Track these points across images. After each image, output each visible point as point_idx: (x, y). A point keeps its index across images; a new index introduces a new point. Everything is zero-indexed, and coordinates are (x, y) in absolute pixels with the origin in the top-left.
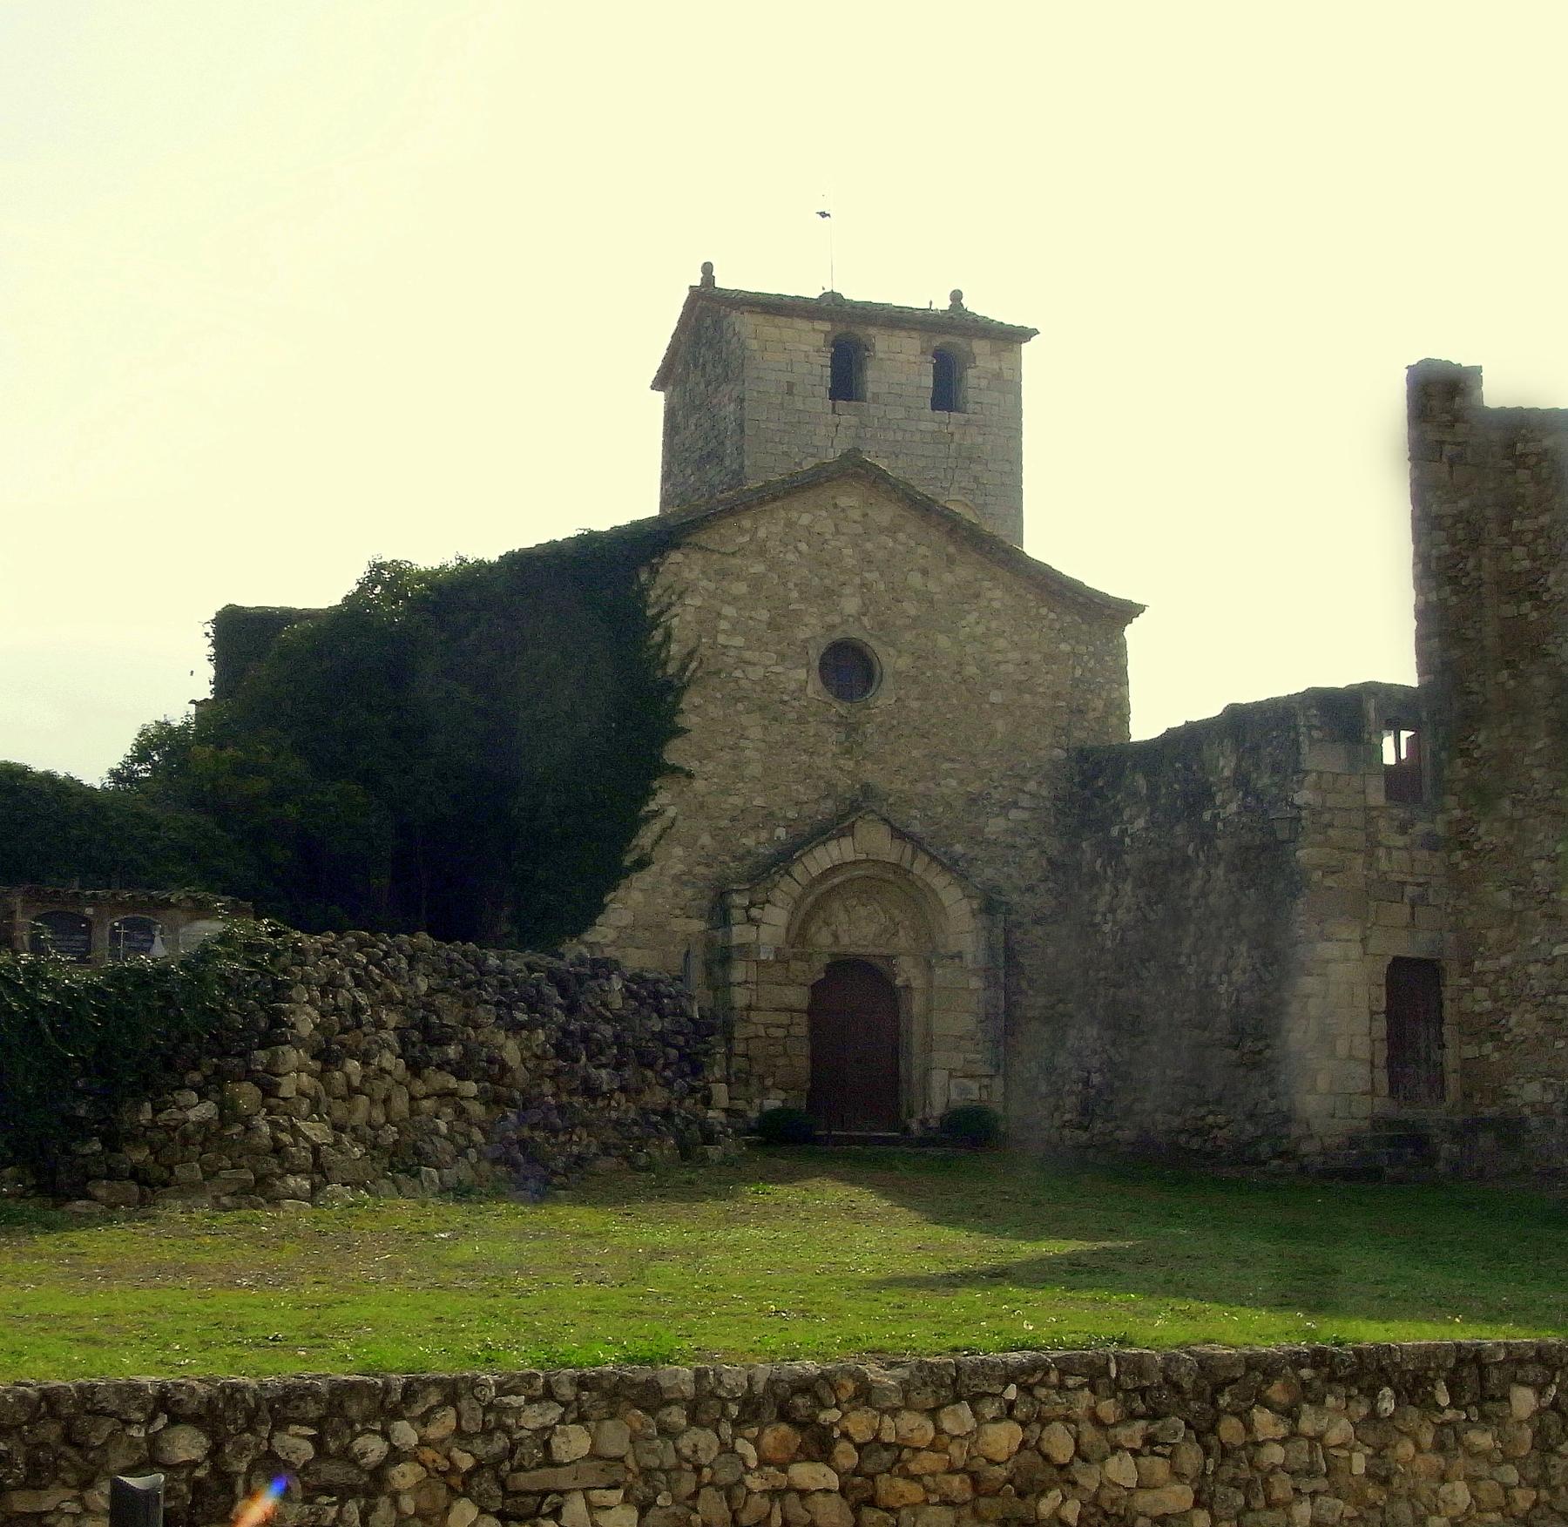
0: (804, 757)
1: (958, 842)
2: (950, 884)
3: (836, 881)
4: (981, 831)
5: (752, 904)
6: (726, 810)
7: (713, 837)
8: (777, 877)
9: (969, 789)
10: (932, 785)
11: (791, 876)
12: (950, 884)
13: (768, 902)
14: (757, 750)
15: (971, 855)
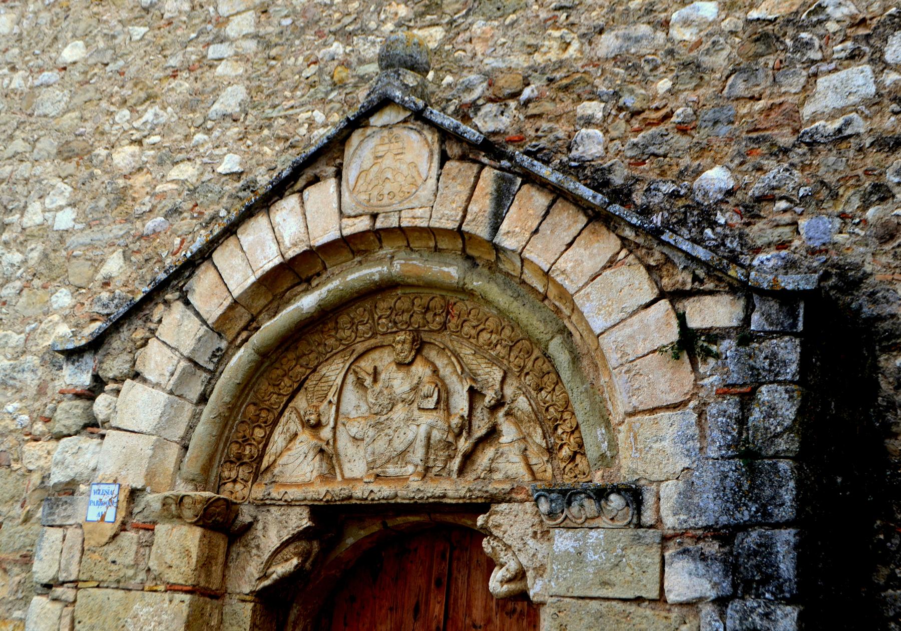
0: (337, 48)
1: (715, 162)
2: (611, 263)
3: (308, 302)
4: (792, 115)
5: (99, 384)
6: (163, 195)
7: (126, 258)
8: (158, 311)
9: (754, 14)
10: (643, 29)
11: (187, 303)
12: (611, 263)
13: (136, 376)
14: (239, 57)
15: (756, 189)
